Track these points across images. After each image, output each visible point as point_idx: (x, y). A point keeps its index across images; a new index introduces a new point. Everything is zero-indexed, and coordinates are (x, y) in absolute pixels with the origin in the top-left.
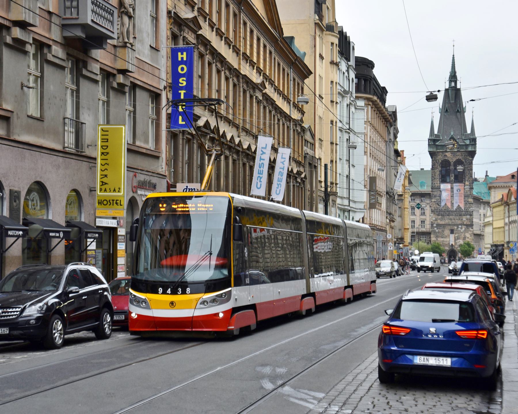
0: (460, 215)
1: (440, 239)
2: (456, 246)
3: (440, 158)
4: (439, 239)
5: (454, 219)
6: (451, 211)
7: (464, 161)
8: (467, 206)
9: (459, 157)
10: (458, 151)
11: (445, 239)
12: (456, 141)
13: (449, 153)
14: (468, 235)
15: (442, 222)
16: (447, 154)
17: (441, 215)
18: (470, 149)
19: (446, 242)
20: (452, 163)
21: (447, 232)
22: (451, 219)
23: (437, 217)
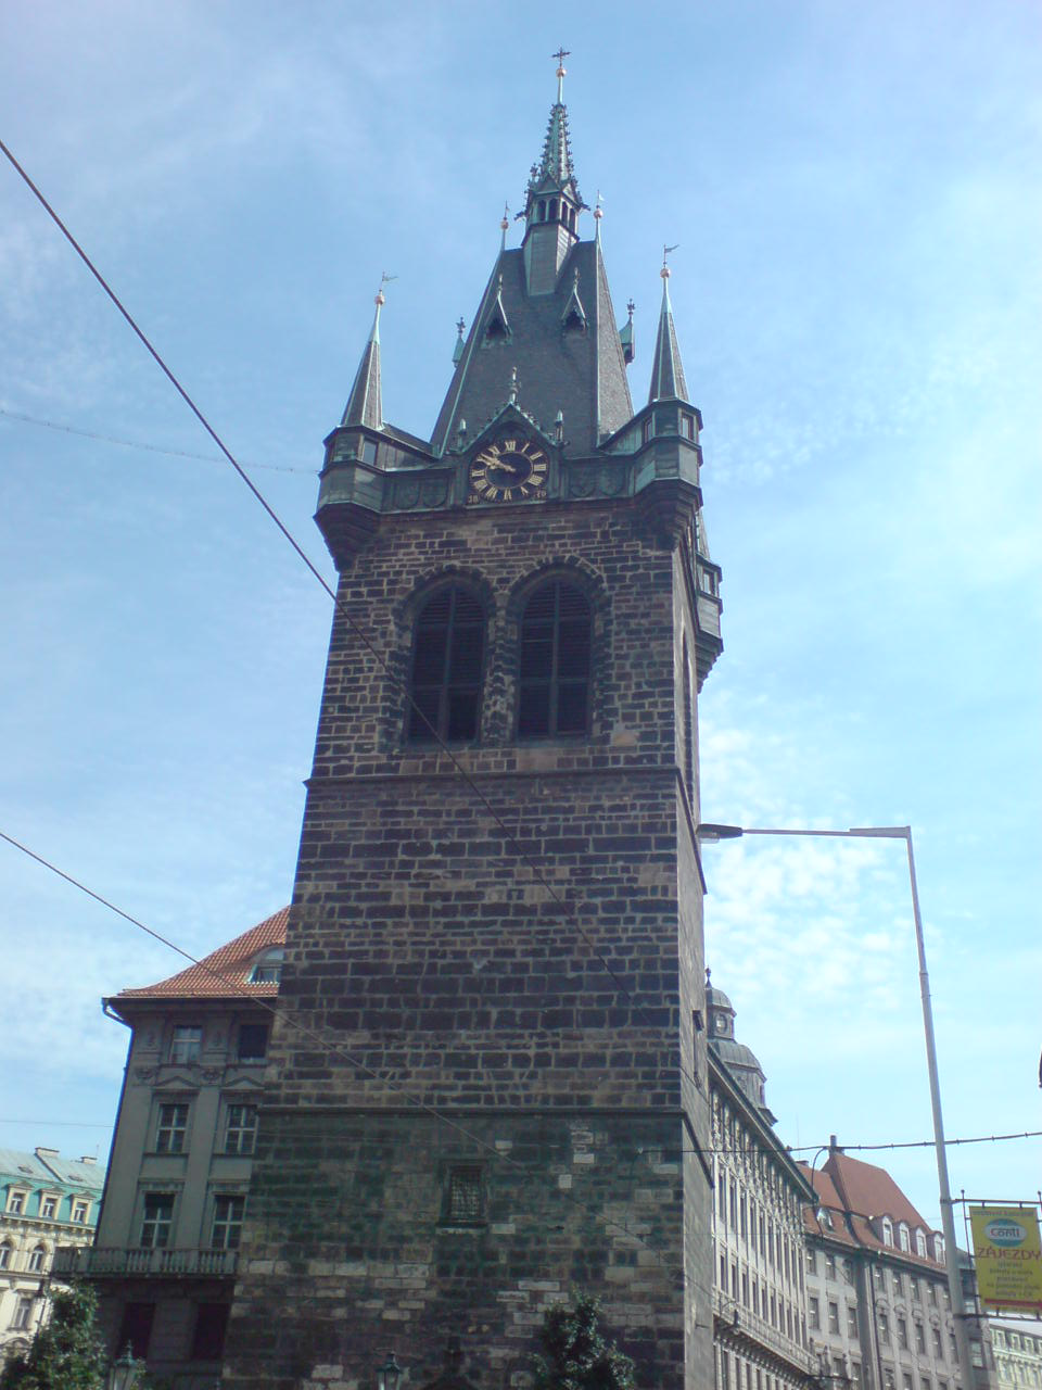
0: (552, 1021)
1: (336, 1272)
2: (497, 1353)
3: (408, 560)
4: (319, 1268)
5: (494, 1061)
6: (472, 985)
7: (598, 570)
8: (625, 933)
9: (562, 542)
10: (554, 506)
11: (385, 1274)
12: (538, 443)
13: (485, 525)
14: (622, 1226)
15: (378, 1093)
16: (465, 533)
17: (372, 1022)
18: (646, 476)
19: (394, 1296)
20: (502, 595)
21: (410, 1196)
22: (461, 1063)
23: (323, 1040)
